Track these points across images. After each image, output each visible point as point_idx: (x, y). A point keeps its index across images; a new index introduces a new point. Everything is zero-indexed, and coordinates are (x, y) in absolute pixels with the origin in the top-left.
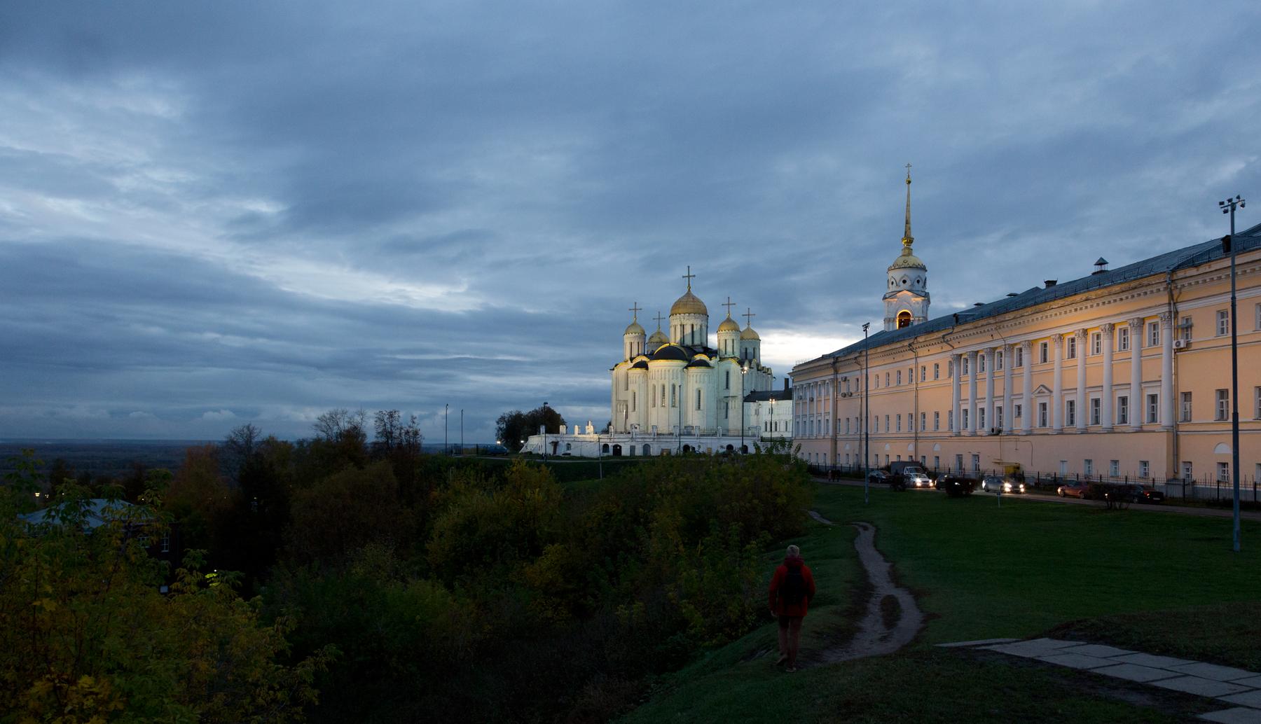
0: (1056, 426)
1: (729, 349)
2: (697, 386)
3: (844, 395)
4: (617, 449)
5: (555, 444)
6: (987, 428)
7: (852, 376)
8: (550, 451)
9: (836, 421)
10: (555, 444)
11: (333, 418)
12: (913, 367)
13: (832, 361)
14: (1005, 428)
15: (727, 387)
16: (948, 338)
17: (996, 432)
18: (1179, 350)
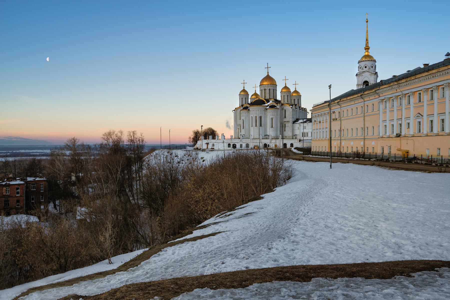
0: (425, 132)
1: (286, 100)
2: (271, 117)
3: (334, 120)
4: (234, 146)
5: (208, 144)
6: (395, 134)
7: (337, 111)
9: (331, 131)
10: (208, 144)
11: (110, 134)
12: (363, 106)
13: (328, 104)
14: (403, 134)
15: (285, 117)
16: (377, 92)
17: (398, 136)
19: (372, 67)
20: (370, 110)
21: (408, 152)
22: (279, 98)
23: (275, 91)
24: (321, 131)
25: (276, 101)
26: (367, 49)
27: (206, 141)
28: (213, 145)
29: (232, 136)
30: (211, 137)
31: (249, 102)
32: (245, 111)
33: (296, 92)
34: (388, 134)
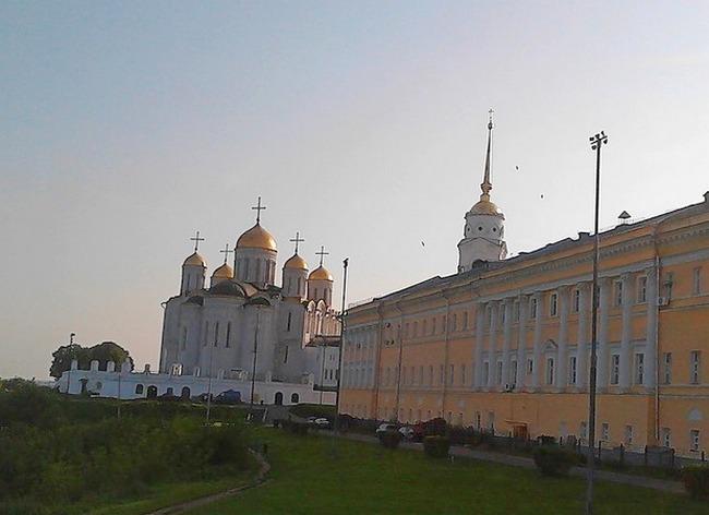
4: (152, 391)
5: (84, 382)
8: (75, 390)
9: (379, 369)
10: (84, 382)
18: (665, 307)
19: (495, 230)
20: (460, 328)
21: (526, 428)
22: (278, 283)
23: (270, 265)
24: (359, 368)
25: (272, 287)
26: (486, 187)
27: (82, 374)
28: (99, 385)
29: (147, 367)
30: (95, 364)
31: (207, 285)
32: (192, 306)
33: (320, 272)
34: (489, 385)
